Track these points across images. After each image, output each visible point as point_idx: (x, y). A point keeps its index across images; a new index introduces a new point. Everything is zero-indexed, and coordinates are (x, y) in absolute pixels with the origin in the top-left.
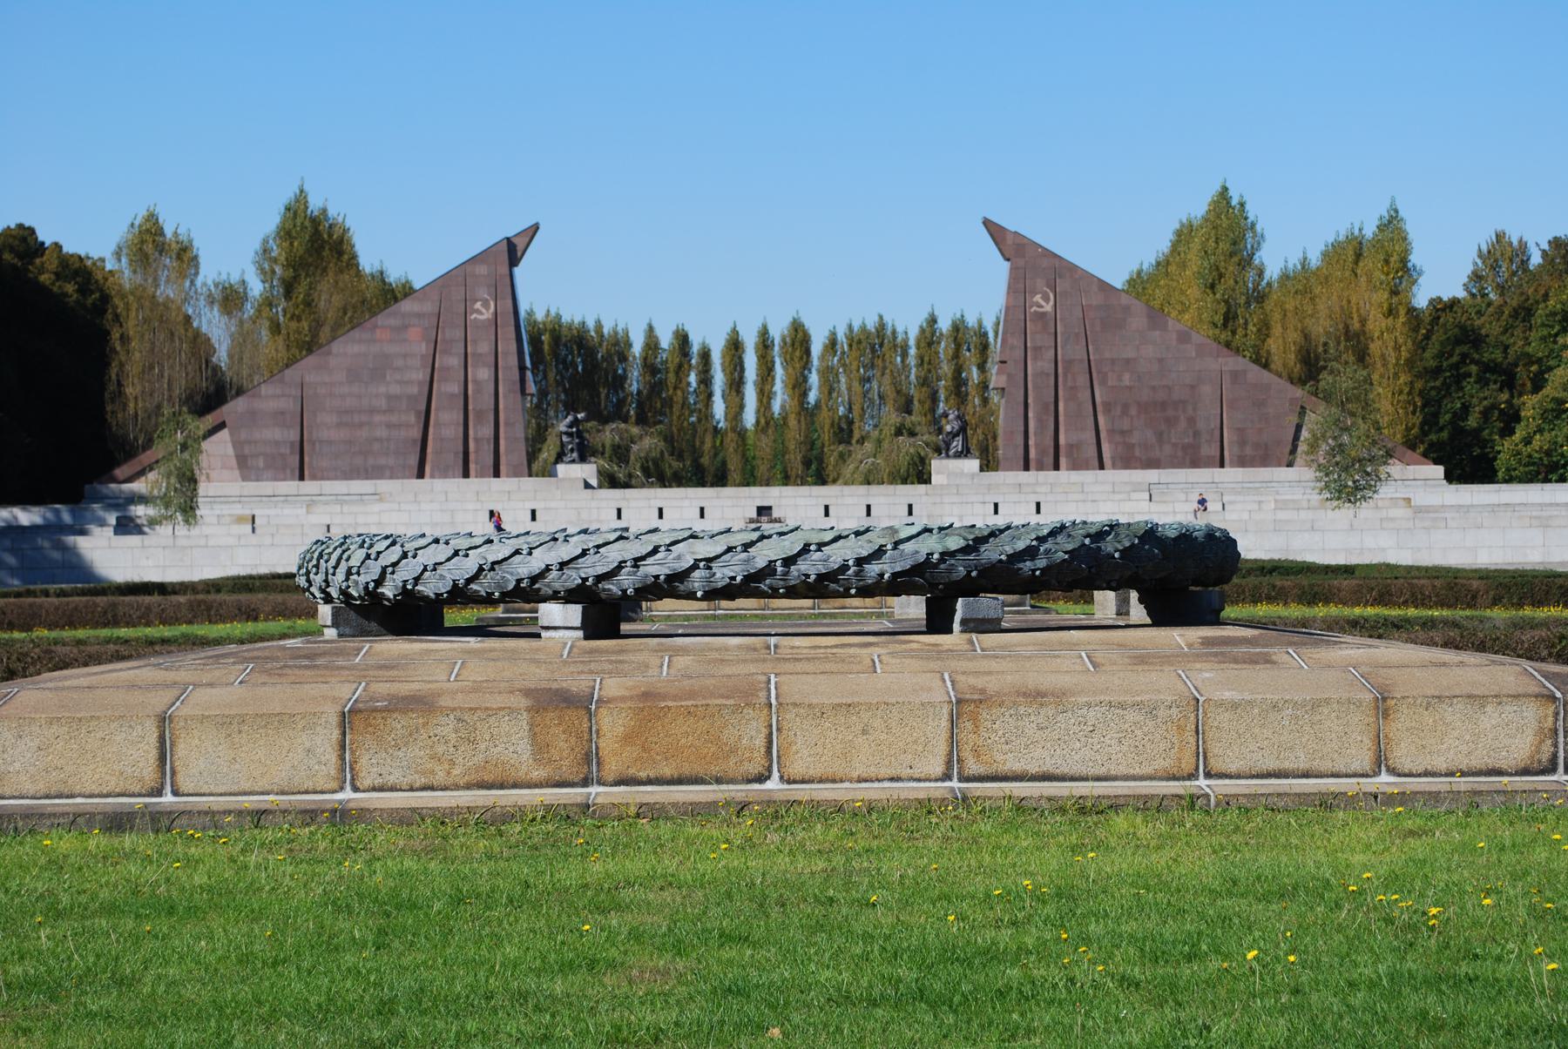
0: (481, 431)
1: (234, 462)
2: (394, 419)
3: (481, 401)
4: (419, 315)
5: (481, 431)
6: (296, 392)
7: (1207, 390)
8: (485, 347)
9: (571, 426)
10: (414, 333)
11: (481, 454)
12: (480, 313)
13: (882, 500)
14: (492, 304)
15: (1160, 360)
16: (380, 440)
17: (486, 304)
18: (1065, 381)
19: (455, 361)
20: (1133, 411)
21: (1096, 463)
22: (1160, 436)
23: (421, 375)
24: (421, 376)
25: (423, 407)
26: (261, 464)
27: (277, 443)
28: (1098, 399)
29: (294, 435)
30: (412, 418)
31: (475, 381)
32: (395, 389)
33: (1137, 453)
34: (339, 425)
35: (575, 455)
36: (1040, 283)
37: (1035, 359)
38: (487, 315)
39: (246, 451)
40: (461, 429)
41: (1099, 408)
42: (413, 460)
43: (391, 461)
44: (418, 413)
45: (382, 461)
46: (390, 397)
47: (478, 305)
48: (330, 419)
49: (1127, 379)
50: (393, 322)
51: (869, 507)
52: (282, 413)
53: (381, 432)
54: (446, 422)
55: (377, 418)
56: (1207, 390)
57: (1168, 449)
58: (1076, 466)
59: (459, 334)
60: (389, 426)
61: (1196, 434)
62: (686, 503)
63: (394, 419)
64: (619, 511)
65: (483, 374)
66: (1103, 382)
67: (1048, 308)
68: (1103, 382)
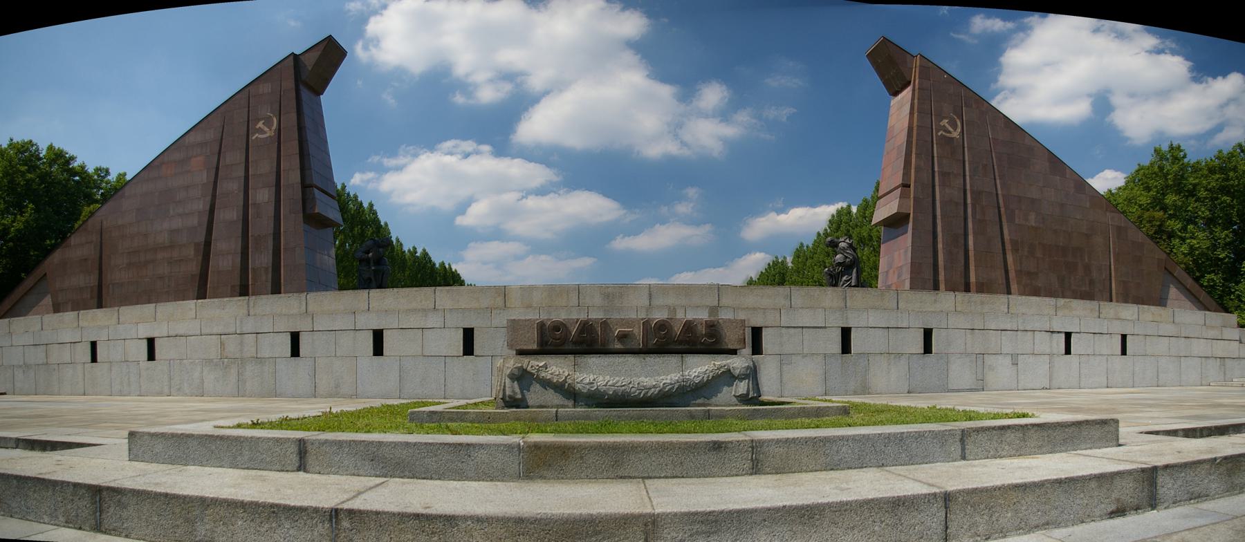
13: (874, 318)
17: (268, 123)
18: (974, 217)
23: (201, 205)
28: (1007, 237)
32: (177, 223)
37: (943, 185)
38: (269, 133)
41: (1008, 246)
47: (260, 125)
51: (846, 333)
59: (239, 157)
62: (433, 320)
64: (295, 338)
66: (1011, 219)
68: (1011, 219)
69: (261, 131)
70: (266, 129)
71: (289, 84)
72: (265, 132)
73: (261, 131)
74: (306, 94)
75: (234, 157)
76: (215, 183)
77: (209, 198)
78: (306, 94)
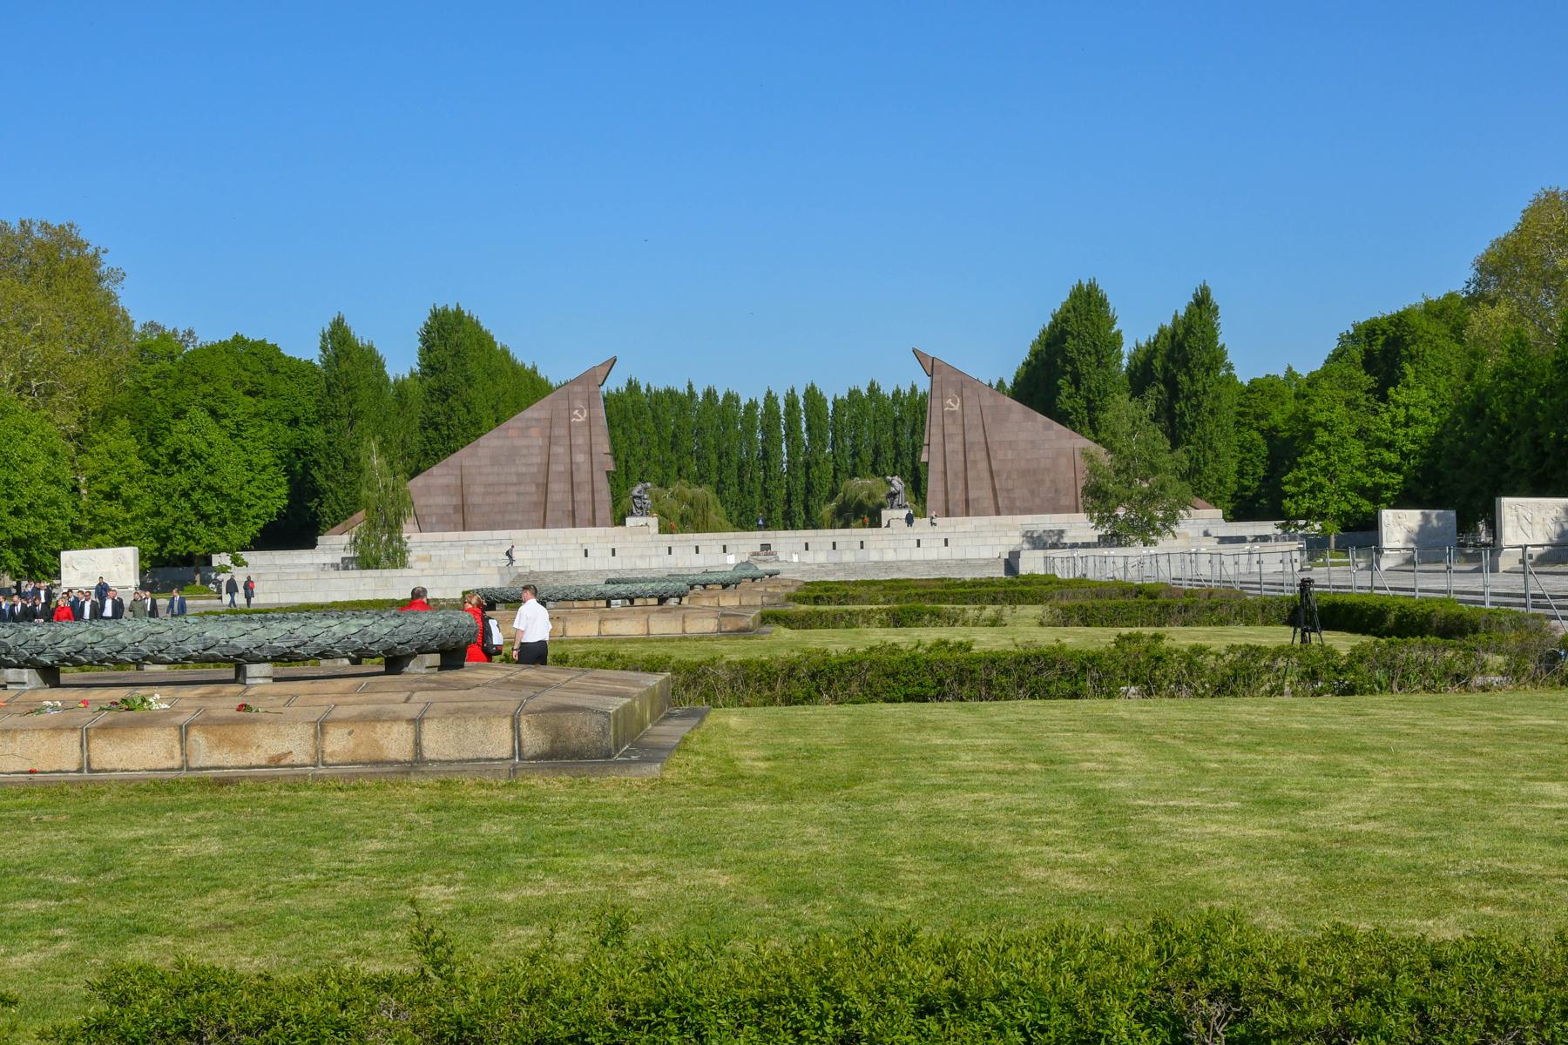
0: (583, 496)
2: (522, 489)
3: (582, 476)
4: (537, 420)
5: (583, 496)
7: (1063, 461)
8: (580, 440)
10: (534, 432)
11: (584, 511)
15: (1032, 442)
17: (581, 412)
19: (559, 450)
20: (1015, 476)
21: (993, 510)
22: (1032, 493)
25: (541, 480)
29: (456, 500)
30: (533, 489)
33: (1018, 504)
36: (951, 392)
44: (538, 485)
45: (514, 517)
46: (518, 474)
48: (479, 489)
49: (1010, 455)
50: (519, 424)
53: (513, 498)
54: (558, 489)
55: (512, 489)
56: (1063, 461)
57: (1038, 501)
58: (977, 514)
59: (563, 432)
60: (518, 494)
61: (1056, 491)
63: (522, 489)
65: (580, 458)
67: (957, 408)
75: (560, 431)
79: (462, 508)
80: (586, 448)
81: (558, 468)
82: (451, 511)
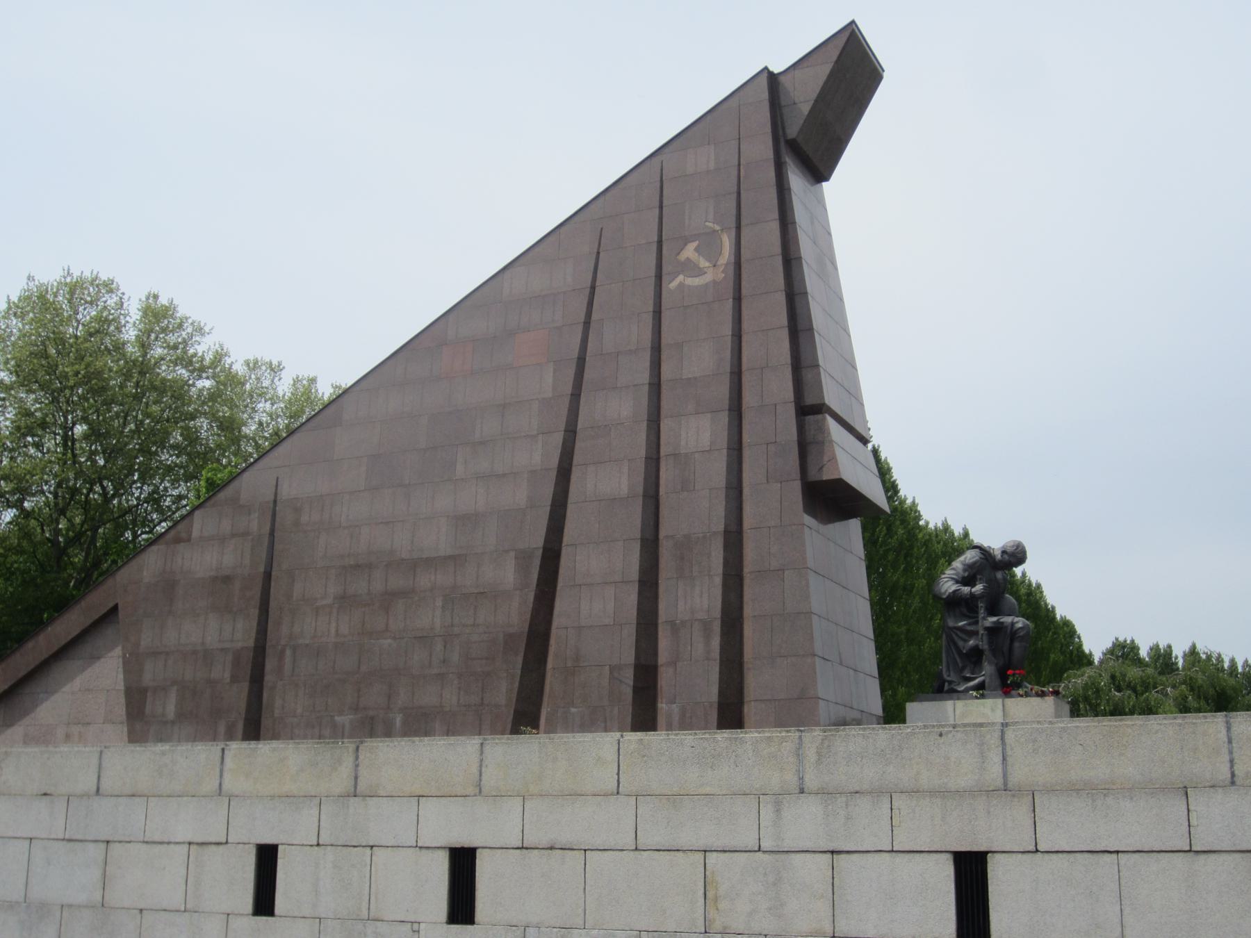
0: (692, 599)
1: (120, 710)
3: (694, 512)
5: (692, 599)
6: (255, 523)
9: (968, 581)
12: (701, 272)
14: (727, 243)
16: (423, 639)
17: (708, 244)
23: (540, 455)
24: (537, 458)
26: (171, 710)
27: (206, 656)
29: (241, 633)
31: (676, 456)
34: (345, 601)
35: (988, 671)
39: (147, 678)
40: (631, 597)
42: (503, 693)
43: (450, 697)
44: (523, 557)
46: (465, 521)
47: (689, 252)
52: (227, 579)
53: (431, 618)
65: (696, 434)
69: (690, 268)
70: (704, 263)
71: (761, 148)
72: (700, 271)
73: (690, 268)
74: (796, 181)
75: (623, 334)
76: (576, 396)
77: (558, 438)
78: (796, 181)
79: (256, 667)
80: (722, 391)
81: (607, 481)
82: (221, 671)
